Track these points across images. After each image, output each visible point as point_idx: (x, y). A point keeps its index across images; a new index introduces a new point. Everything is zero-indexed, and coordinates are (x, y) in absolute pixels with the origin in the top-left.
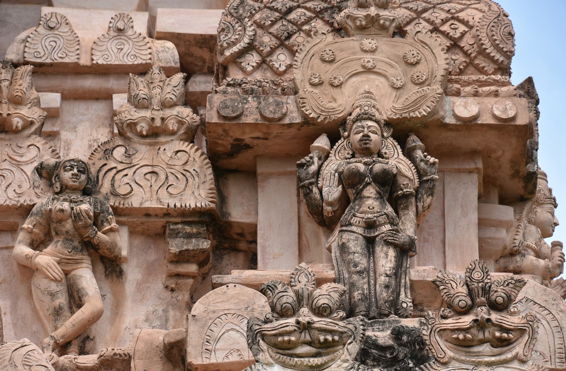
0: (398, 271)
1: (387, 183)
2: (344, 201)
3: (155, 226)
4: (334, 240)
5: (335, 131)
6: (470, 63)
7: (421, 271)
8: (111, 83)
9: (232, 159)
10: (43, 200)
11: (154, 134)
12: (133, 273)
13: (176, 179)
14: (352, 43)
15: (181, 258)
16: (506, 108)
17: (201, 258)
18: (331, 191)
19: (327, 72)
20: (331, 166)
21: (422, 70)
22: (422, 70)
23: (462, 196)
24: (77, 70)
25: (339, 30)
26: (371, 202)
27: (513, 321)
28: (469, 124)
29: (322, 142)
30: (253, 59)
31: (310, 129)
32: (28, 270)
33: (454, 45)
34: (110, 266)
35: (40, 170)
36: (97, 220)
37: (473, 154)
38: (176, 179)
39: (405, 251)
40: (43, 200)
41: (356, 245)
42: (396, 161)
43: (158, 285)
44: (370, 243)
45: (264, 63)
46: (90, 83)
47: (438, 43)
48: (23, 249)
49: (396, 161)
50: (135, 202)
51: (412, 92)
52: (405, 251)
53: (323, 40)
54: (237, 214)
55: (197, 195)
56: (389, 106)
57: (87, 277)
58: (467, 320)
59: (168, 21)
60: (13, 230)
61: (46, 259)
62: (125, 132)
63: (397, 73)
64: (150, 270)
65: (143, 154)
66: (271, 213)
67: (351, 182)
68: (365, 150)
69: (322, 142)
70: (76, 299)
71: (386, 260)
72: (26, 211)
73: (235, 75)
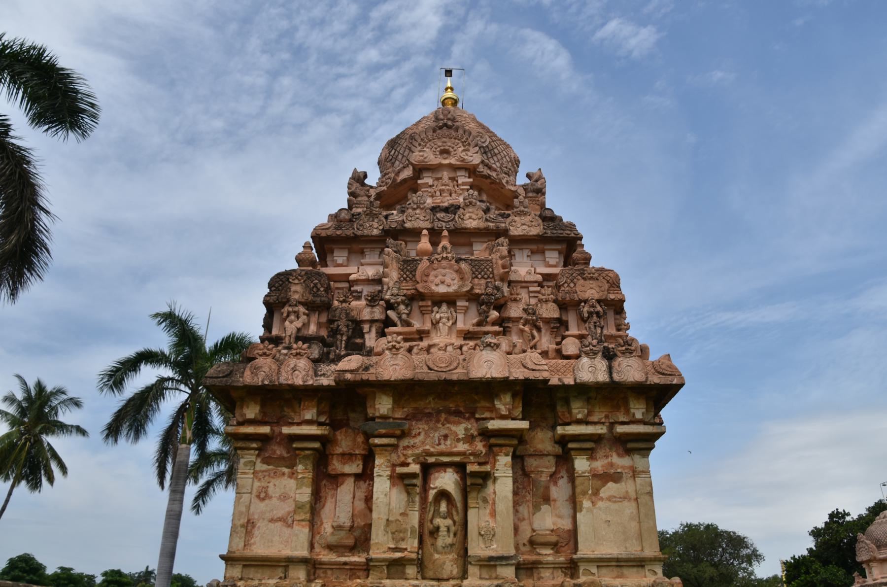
0: (602, 332)
1: (598, 313)
2: (588, 317)
3: (547, 321)
4: (587, 325)
5: (585, 301)
6: (611, 286)
7: (605, 332)
8: (528, 285)
9: (563, 306)
10: (525, 316)
11: (547, 301)
12: (543, 331)
13: (550, 311)
14: (588, 282)
15: (554, 328)
16: (619, 297)
17: (557, 328)
18: (586, 315)
19: (583, 289)
20: (586, 309)
21: (603, 289)
22: (603, 289)
23: (611, 316)
24: (521, 282)
25: (585, 279)
26: (595, 318)
27: (633, 348)
28: (613, 300)
29: (583, 304)
30: (566, 285)
31: (580, 301)
32: (522, 331)
33: (608, 282)
34: (539, 330)
35: (523, 309)
36: (537, 320)
37: (612, 305)
38: (550, 311)
39: (602, 328)
40: (525, 316)
41: (592, 327)
42: (599, 308)
43: (548, 333)
44: (595, 327)
45: (568, 286)
46: (524, 285)
47: (605, 282)
48: (522, 327)
49: (599, 308)
50: (545, 315)
51: (601, 293)
52: (602, 328)
53: (582, 281)
54: (564, 318)
55: (556, 315)
56: (597, 296)
57: (535, 333)
58: (624, 348)
59: (539, 270)
60: (518, 322)
61: (527, 328)
62: (540, 301)
63: (598, 289)
64: (546, 330)
65: (544, 305)
66: (572, 319)
67: (590, 314)
68: (593, 306)
69: (583, 304)
70: (533, 337)
71: (599, 331)
72: (521, 318)
73: (562, 289)
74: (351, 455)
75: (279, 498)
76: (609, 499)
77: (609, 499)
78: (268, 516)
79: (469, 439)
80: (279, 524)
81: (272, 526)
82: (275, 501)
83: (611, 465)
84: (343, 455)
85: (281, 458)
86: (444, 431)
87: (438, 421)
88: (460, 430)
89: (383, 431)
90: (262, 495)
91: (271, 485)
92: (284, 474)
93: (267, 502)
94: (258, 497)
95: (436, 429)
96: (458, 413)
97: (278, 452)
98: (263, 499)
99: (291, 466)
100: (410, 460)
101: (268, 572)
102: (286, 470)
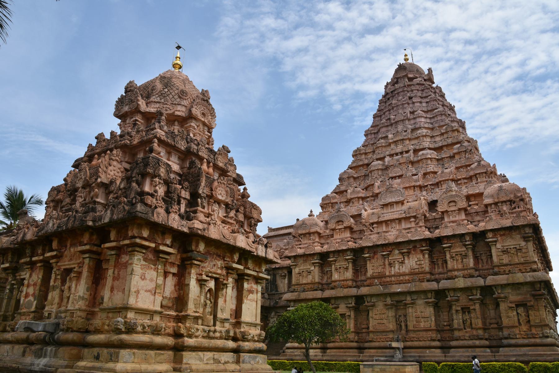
74: (174, 264)
75: (150, 280)
76: (250, 300)
77: (250, 300)
78: (145, 288)
79: (222, 268)
80: (149, 293)
81: (146, 293)
82: (148, 281)
83: (252, 287)
84: (171, 263)
85: (151, 260)
86: (214, 263)
87: (213, 258)
88: (220, 263)
89: (199, 259)
90: (143, 277)
91: (146, 273)
92: (152, 268)
93: (144, 281)
94: (141, 278)
95: (212, 261)
96: (219, 256)
97: (150, 256)
98: (143, 280)
99: (155, 265)
100: (203, 273)
101: (143, 316)
102: (153, 267)
